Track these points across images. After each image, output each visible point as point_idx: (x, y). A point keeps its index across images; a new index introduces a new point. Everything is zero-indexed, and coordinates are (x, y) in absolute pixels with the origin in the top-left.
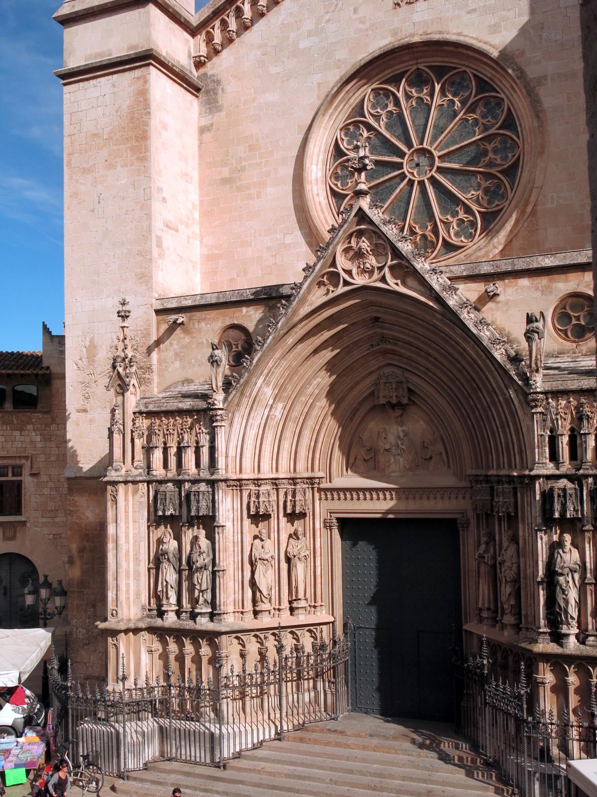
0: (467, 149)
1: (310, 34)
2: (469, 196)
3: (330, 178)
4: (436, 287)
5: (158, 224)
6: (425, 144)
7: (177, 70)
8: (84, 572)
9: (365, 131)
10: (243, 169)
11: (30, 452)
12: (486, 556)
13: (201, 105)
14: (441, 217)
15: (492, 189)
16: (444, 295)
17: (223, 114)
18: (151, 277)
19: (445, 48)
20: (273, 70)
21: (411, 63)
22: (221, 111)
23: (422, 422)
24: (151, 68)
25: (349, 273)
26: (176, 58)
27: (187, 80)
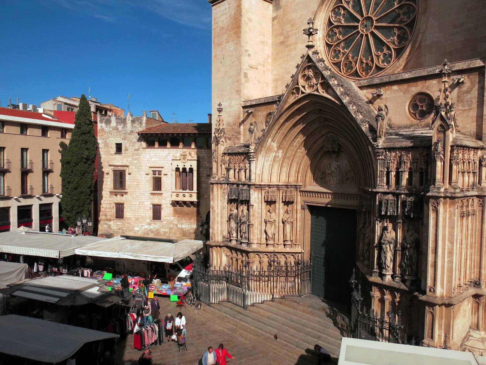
0: (390, 15)
2: (390, 40)
3: (326, 37)
4: (339, 93)
5: (245, 67)
9: (342, 11)
10: (289, 37)
12: (362, 230)
13: (273, 7)
14: (375, 53)
15: (401, 35)
16: (342, 97)
17: (282, 10)
18: (241, 92)
22: (281, 8)
23: (346, 161)
25: (304, 87)
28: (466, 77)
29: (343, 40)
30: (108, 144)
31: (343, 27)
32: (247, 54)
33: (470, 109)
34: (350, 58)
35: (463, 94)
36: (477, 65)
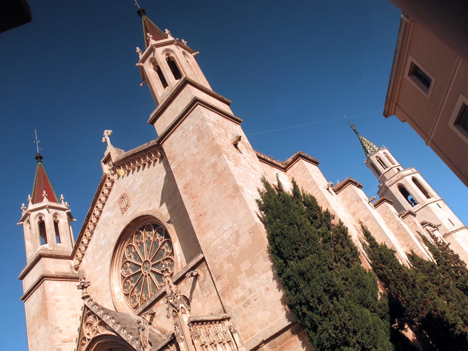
0: (158, 253)
4: (111, 325)
6: (146, 259)
7: (61, 276)
19: (139, 220)
20: (97, 258)
21: (134, 231)
24: (45, 281)
25: (88, 334)
26: (62, 271)
27: (70, 277)
28: (199, 270)
29: (135, 286)
31: (132, 276)
32: (58, 331)
33: (211, 292)
34: (144, 298)
35: (202, 283)
36: (200, 259)
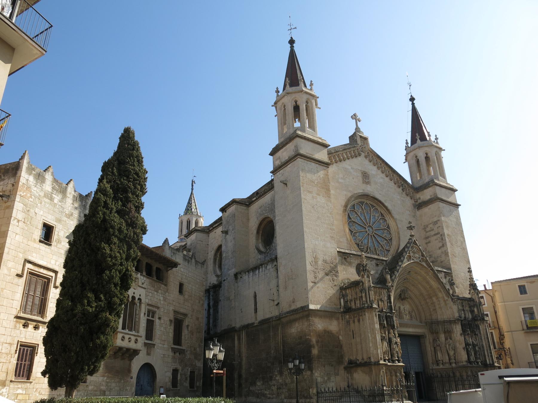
1: (342, 178)
8: (319, 351)
11: (159, 305)
30: (32, 218)
